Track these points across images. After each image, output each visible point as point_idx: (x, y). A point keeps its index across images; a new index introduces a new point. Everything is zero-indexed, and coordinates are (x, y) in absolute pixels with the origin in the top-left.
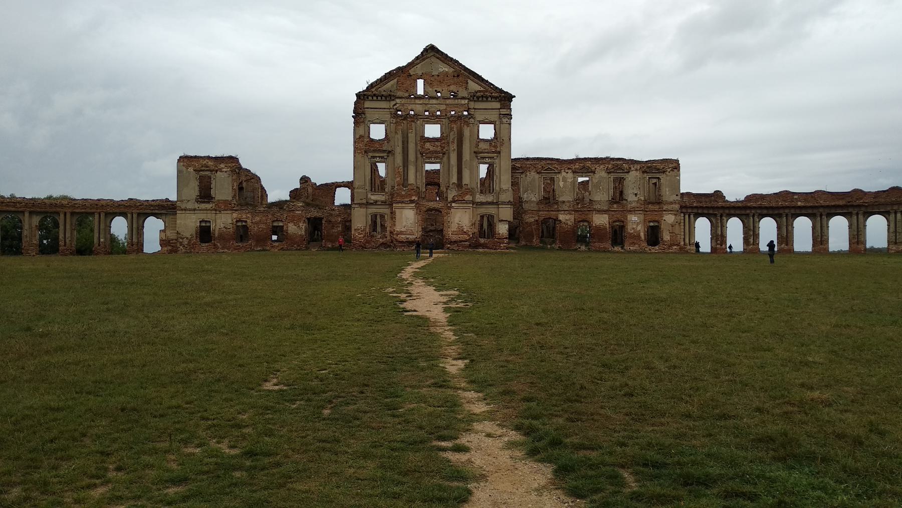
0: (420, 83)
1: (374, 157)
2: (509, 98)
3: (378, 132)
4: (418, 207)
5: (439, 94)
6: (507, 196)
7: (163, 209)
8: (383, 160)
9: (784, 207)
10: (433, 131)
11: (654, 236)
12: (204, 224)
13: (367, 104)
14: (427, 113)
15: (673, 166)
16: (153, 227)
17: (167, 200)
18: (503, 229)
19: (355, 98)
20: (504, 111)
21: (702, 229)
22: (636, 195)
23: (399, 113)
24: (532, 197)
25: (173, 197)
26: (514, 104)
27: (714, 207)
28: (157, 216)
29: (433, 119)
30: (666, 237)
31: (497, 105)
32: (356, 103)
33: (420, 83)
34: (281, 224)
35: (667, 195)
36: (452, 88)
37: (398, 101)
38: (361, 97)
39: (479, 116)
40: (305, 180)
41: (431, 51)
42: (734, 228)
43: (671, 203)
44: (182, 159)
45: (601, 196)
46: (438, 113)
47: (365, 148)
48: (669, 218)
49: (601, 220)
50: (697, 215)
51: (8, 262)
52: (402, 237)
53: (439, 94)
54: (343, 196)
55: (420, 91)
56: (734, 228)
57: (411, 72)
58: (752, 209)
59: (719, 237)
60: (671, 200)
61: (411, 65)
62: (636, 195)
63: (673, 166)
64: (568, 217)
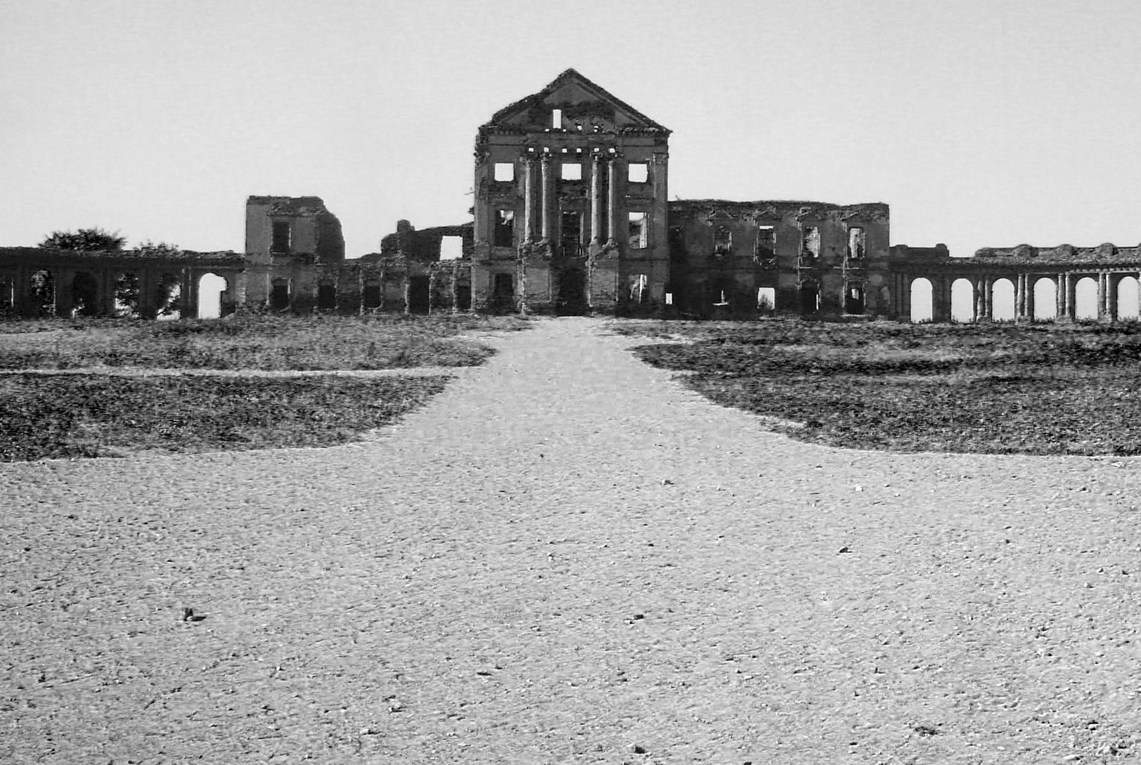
0: (557, 114)
1: (498, 204)
2: (668, 133)
3: (504, 172)
4: (554, 267)
5: (580, 128)
6: (662, 250)
7: (225, 264)
9: (1024, 266)
10: (571, 171)
12: (278, 284)
13: (492, 139)
14: (565, 151)
15: (883, 209)
17: (230, 254)
19: (477, 132)
20: (660, 149)
21: (921, 293)
22: (834, 249)
23: (531, 150)
25: (239, 248)
26: (671, 140)
27: (937, 265)
28: (218, 273)
31: (650, 141)
33: (557, 114)
34: (376, 284)
37: (529, 135)
38: (485, 132)
40: (403, 225)
41: (571, 74)
42: (962, 291)
43: (879, 260)
44: (253, 201)
46: (579, 150)
47: (487, 188)
53: (580, 128)
54: (451, 249)
57: (547, 101)
59: (942, 304)
60: (877, 256)
61: (546, 93)
62: (834, 249)
63: (883, 209)
64: (748, 277)
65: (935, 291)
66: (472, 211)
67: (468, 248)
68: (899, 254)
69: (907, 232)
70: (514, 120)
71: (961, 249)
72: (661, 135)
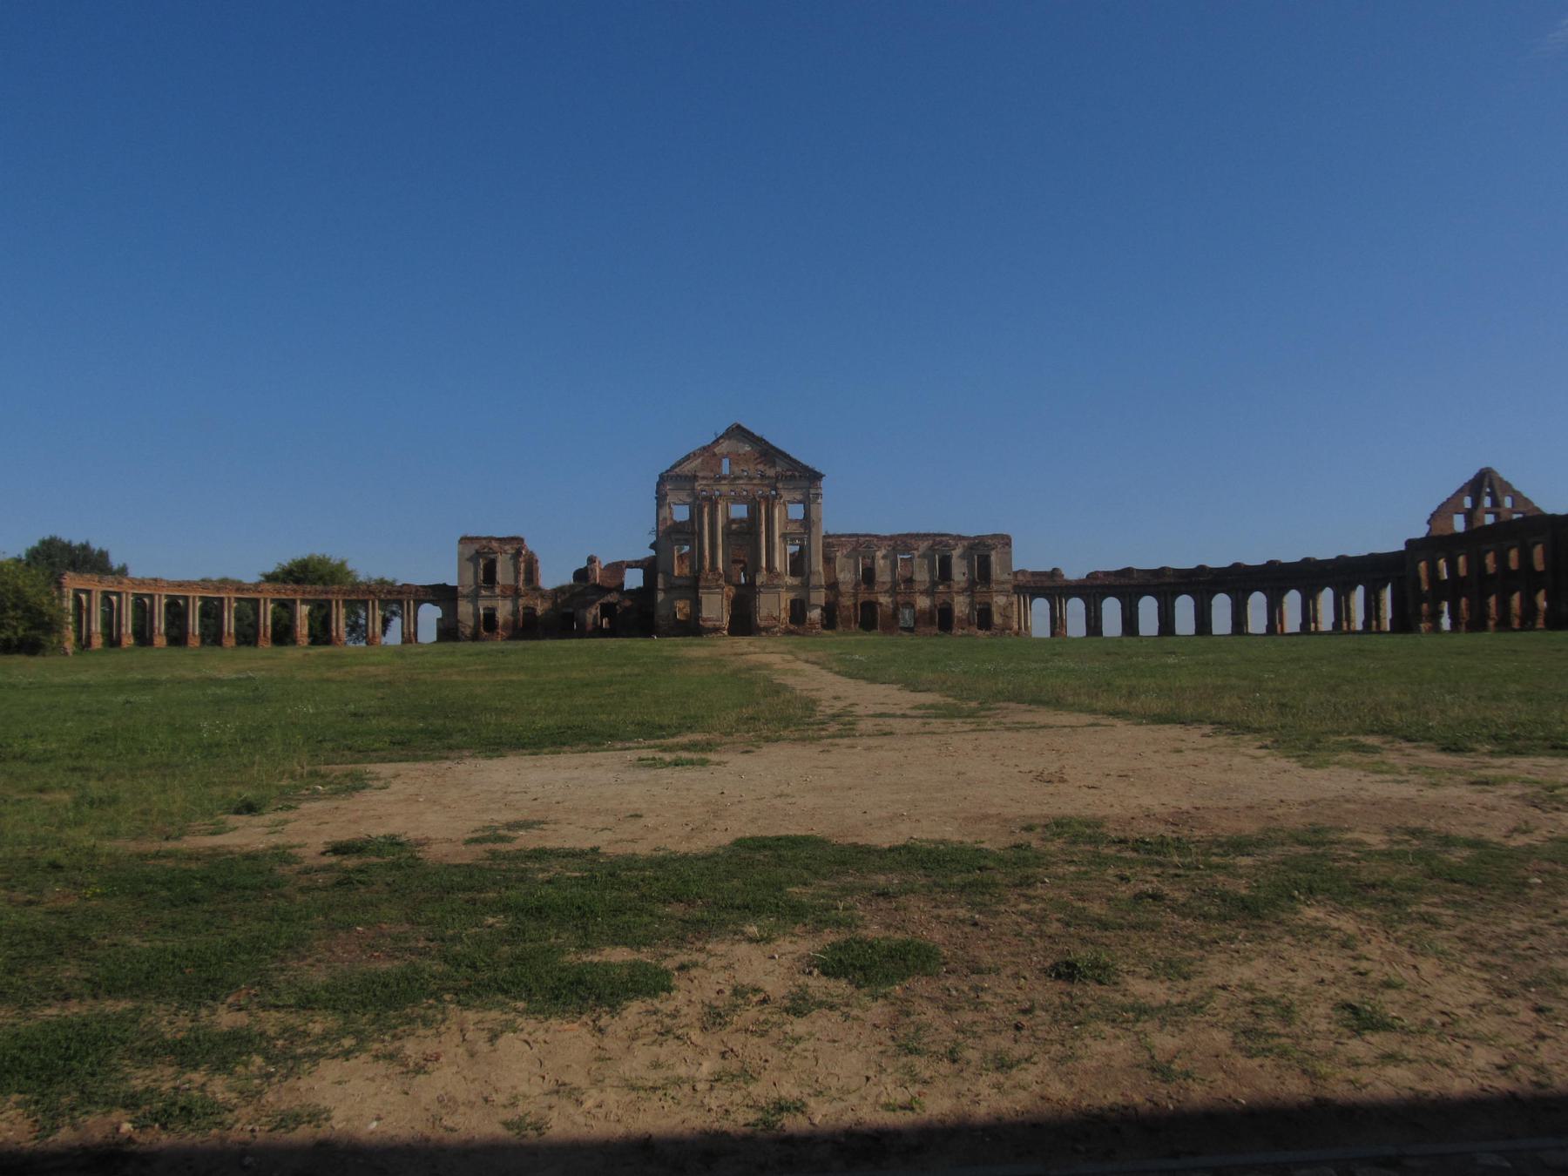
0: (726, 462)
3: (681, 514)
7: (443, 595)
8: (687, 542)
11: (984, 618)
15: (1006, 541)
16: (430, 615)
18: (815, 614)
24: (846, 576)
26: (824, 483)
27: (1052, 587)
29: (737, 500)
30: (997, 619)
32: (658, 484)
33: (726, 462)
35: (996, 571)
36: (760, 467)
38: (663, 479)
39: (786, 496)
44: (465, 540)
45: (922, 576)
48: (1000, 600)
49: (923, 602)
50: (1034, 596)
51: (22, 668)
52: (709, 624)
55: (725, 470)
56: (1075, 608)
58: (1094, 589)
59: (1057, 623)
63: (1006, 541)
65: (1053, 609)
66: (653, 546)
67: (650, 578)
68: (1020, 577)
69: (1028, 558)
70: (688, 468)
71: (1074, 572)
72: (814, 477)
